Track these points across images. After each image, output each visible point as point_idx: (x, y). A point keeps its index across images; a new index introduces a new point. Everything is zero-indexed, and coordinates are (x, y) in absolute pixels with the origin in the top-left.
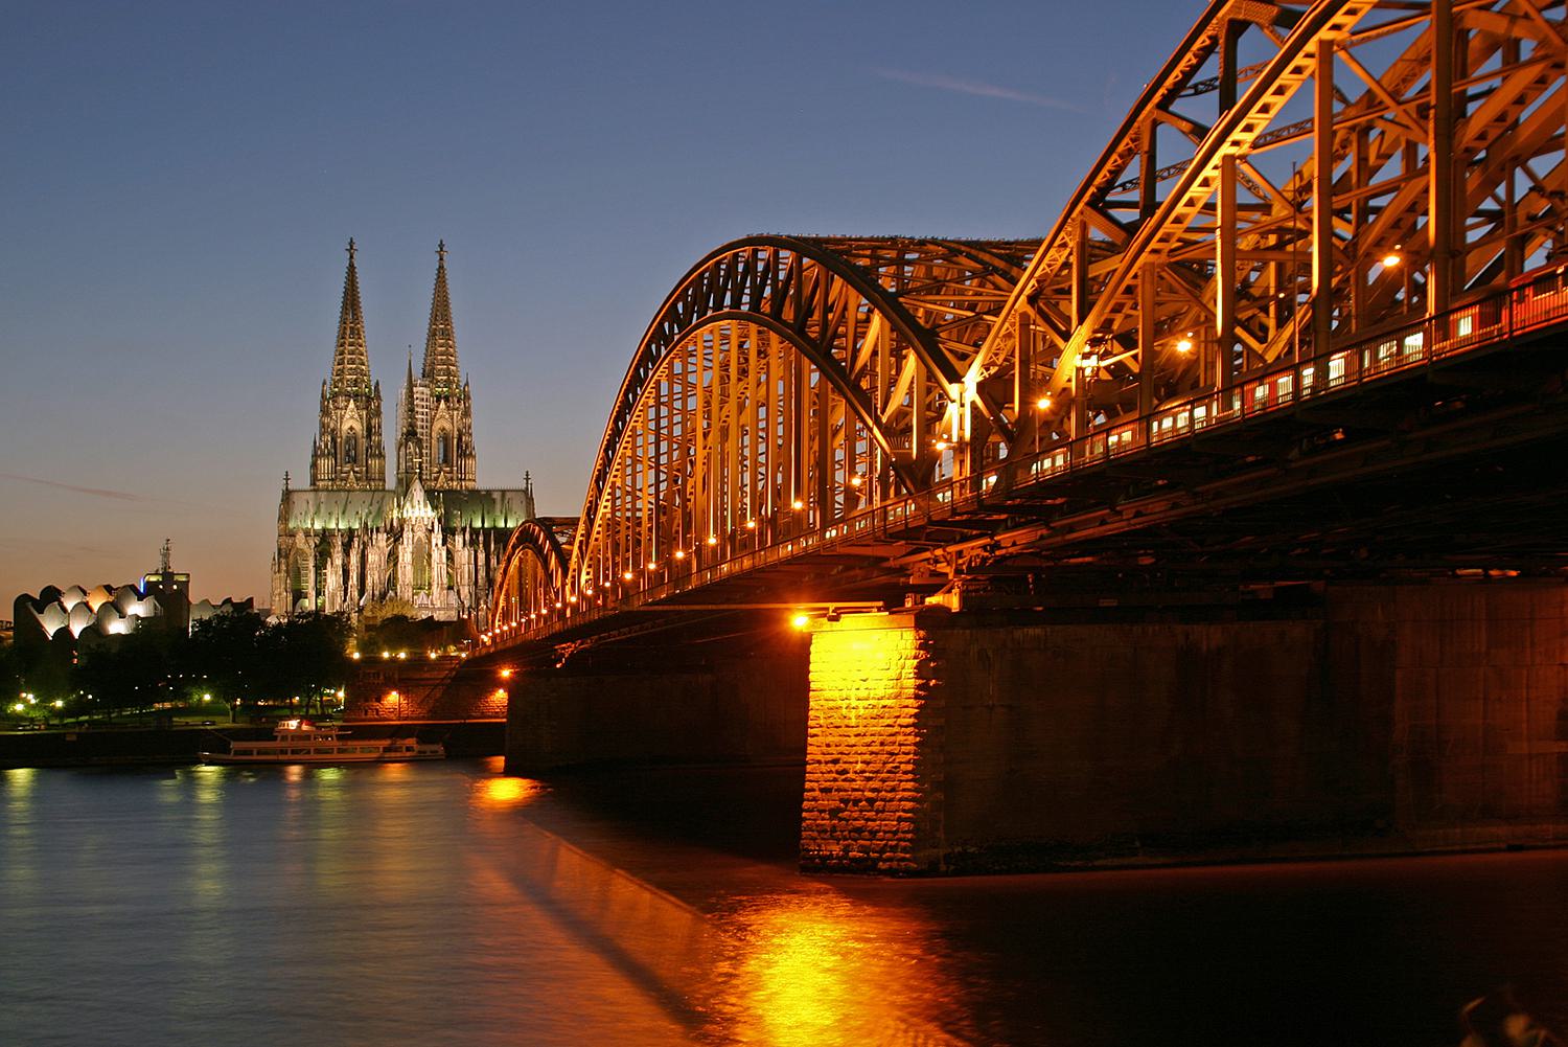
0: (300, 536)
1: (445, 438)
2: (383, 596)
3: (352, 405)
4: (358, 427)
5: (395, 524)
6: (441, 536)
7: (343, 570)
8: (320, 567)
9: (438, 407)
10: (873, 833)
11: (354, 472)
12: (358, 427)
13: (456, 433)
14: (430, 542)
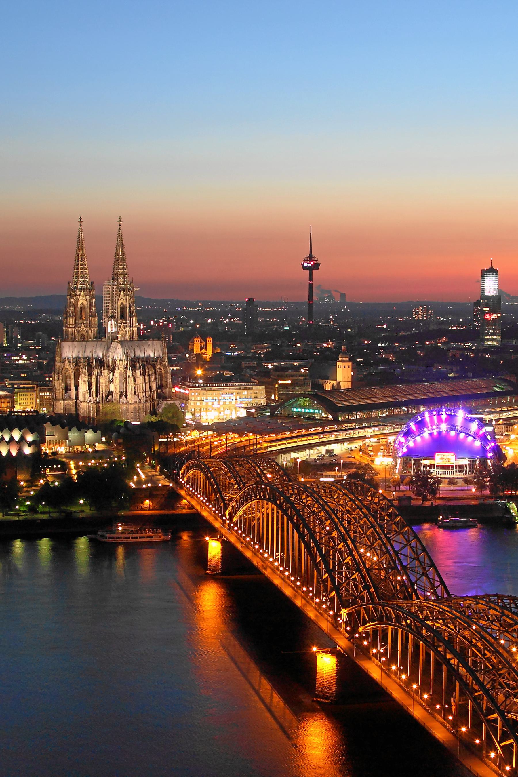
0: (67, 362)
1: (123, 308)
2: (107, 397)
3: (82, 293)
4: (85, 303)
5: (110, 363)
7: (88, 383)
9: (120, 294)
10: (328, 693)
11: (84, 324)
12: (85, 303)
14: (126, 373)
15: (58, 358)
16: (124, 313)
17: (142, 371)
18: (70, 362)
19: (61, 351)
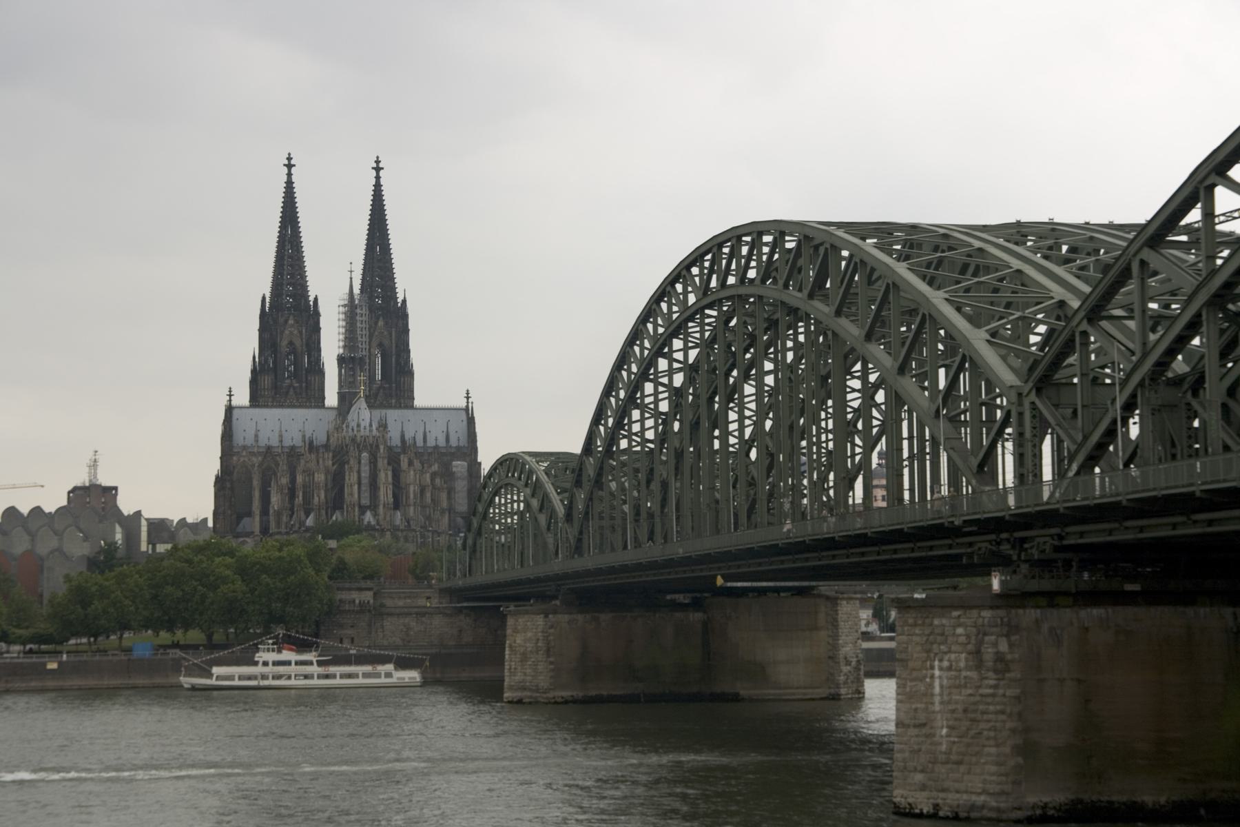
9: (376, 323)
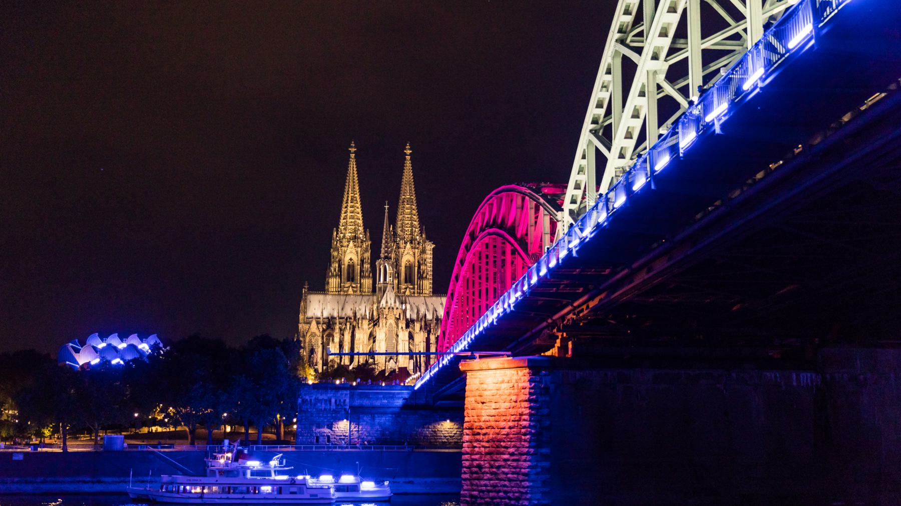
0: (314, 323)
1: (409, 268)
3: (351, 244)
5: (375, 313)
6: (404, 322)
8: (325, 346)
13: (417, 264)
15: (301, 317)
16: (410, 274)
17: (423, 324)
18: (318, 323)
19: (305, 308)
